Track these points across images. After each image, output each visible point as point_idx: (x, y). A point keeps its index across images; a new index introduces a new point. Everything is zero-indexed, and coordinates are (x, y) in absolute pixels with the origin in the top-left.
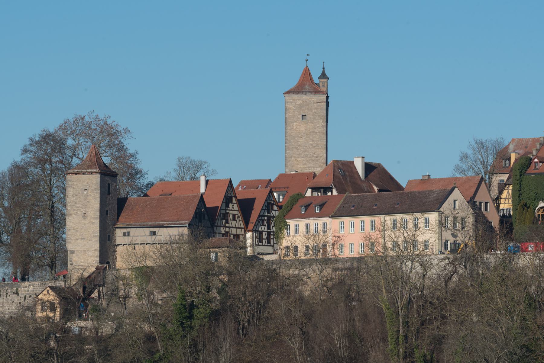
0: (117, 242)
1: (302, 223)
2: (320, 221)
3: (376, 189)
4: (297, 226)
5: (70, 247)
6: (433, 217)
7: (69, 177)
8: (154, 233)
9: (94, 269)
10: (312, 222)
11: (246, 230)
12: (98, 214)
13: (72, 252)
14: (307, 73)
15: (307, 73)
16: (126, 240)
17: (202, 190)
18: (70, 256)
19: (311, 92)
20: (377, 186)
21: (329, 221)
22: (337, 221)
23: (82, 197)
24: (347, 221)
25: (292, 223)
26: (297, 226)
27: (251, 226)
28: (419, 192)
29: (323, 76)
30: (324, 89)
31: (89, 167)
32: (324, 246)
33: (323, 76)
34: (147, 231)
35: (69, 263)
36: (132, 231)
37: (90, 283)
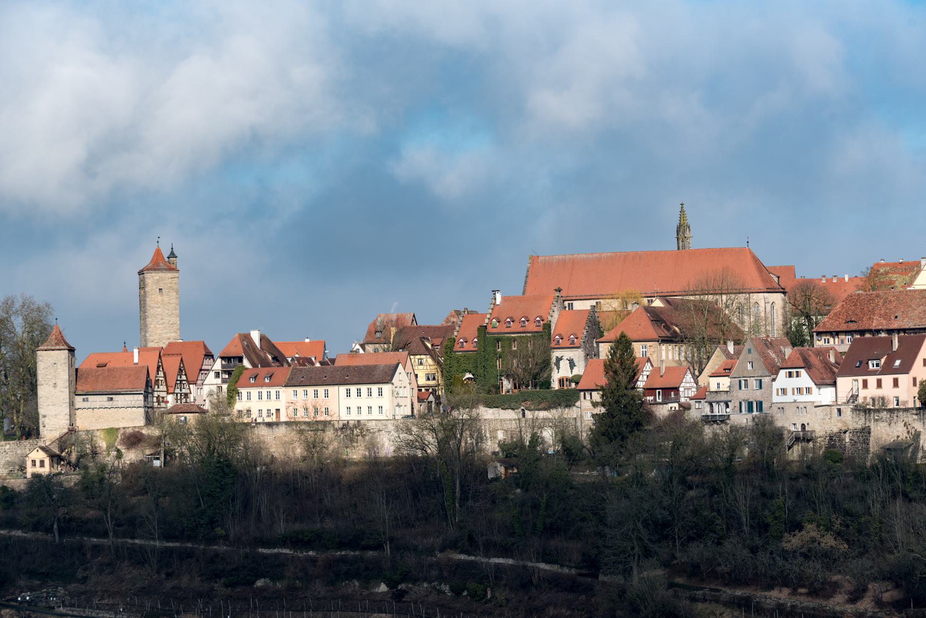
0: (77, 407)
1: (254, 392)
2: (273, 390)
3: (270, 357)
4: (249, 394)
5: (42, 411)
6: (386, 388)
7: (39, 353)
8: (111, 399)
9: (66, 431)
10: (264, 390)
11: (168, 393)
12: (67, 384)
13: (44, 416)
14: (158, 253)
15: (158, 253)
16: (86, 405)
17: (136, 360)
18: (41, 420)
19: (166, 270)
20: (271, 354)
21: (282, 390)
22: (290, 390)
23: (52, 369)
24: (300, 390)
25: (244, 391)
26: (249, 394)
27: (171, 390)
28: (364, 366)
29: (173, 255)
30: (173, 266)
31: (56, 344)
32: (278, 410)
33: (173, 255)
34: (105, 398)
35: (41, 426)
36: (90, 397)
37: (63, 442)
